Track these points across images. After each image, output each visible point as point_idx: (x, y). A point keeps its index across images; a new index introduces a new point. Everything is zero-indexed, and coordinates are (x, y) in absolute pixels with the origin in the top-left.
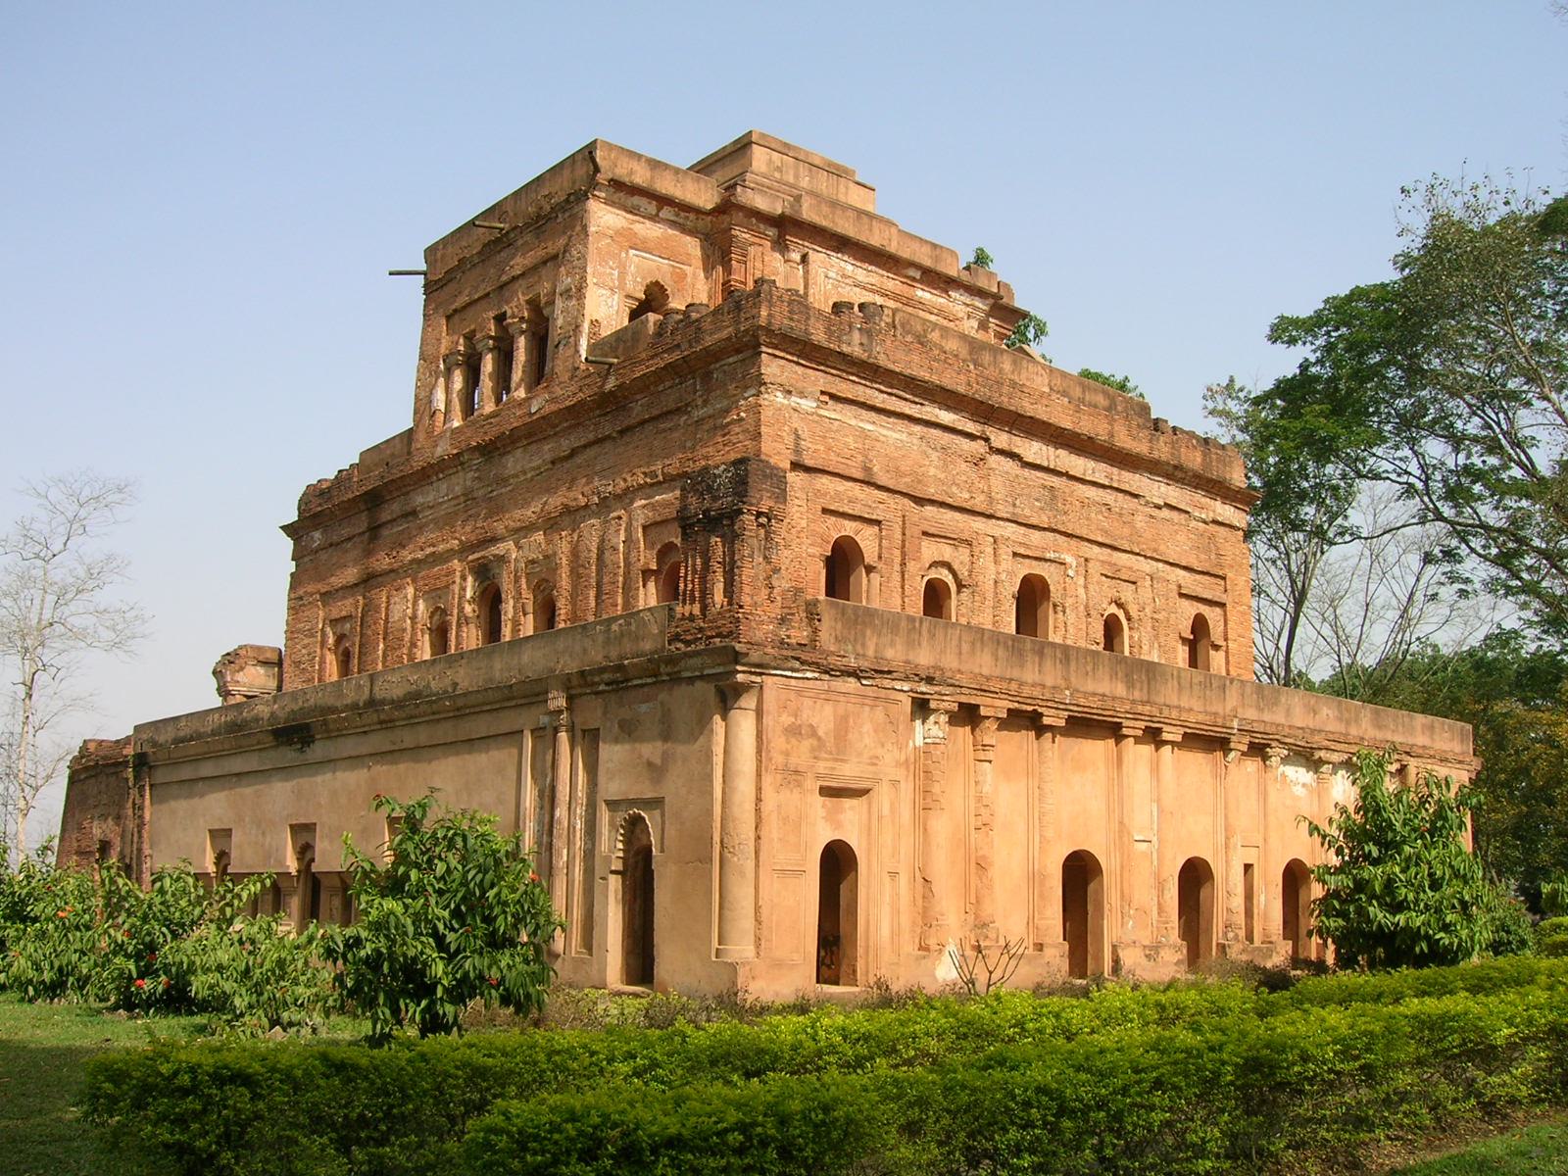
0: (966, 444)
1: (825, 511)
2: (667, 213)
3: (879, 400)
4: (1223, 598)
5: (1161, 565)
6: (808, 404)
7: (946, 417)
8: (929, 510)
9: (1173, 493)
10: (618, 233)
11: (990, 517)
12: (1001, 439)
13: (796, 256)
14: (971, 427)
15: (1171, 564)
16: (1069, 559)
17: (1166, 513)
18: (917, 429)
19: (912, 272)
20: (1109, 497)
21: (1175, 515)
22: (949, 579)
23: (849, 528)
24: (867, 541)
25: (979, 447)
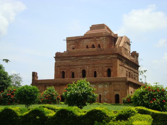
0: (76, 60)
1: (61, 69)
2: (73, 41)
3: (66, 59)
4: (112, 66)
5: (102, 65)
6: (59, 61)
7: (73, 58)
8: (71, 67)
9: (104, 57)
10: (69, 45)
11: (78, 65)
12: (80, 58)
13: (82, 41)
14: (76, 58)
15: (104, 64)
16: (87, 67)
17: (103, 59)
18: (70, 60)
19: (95, 38)
20: (94, 60)
21: (105, 59)
22: (74, 72)
23: (63, 70)
24: (65, 71)
25: (77, 59)
